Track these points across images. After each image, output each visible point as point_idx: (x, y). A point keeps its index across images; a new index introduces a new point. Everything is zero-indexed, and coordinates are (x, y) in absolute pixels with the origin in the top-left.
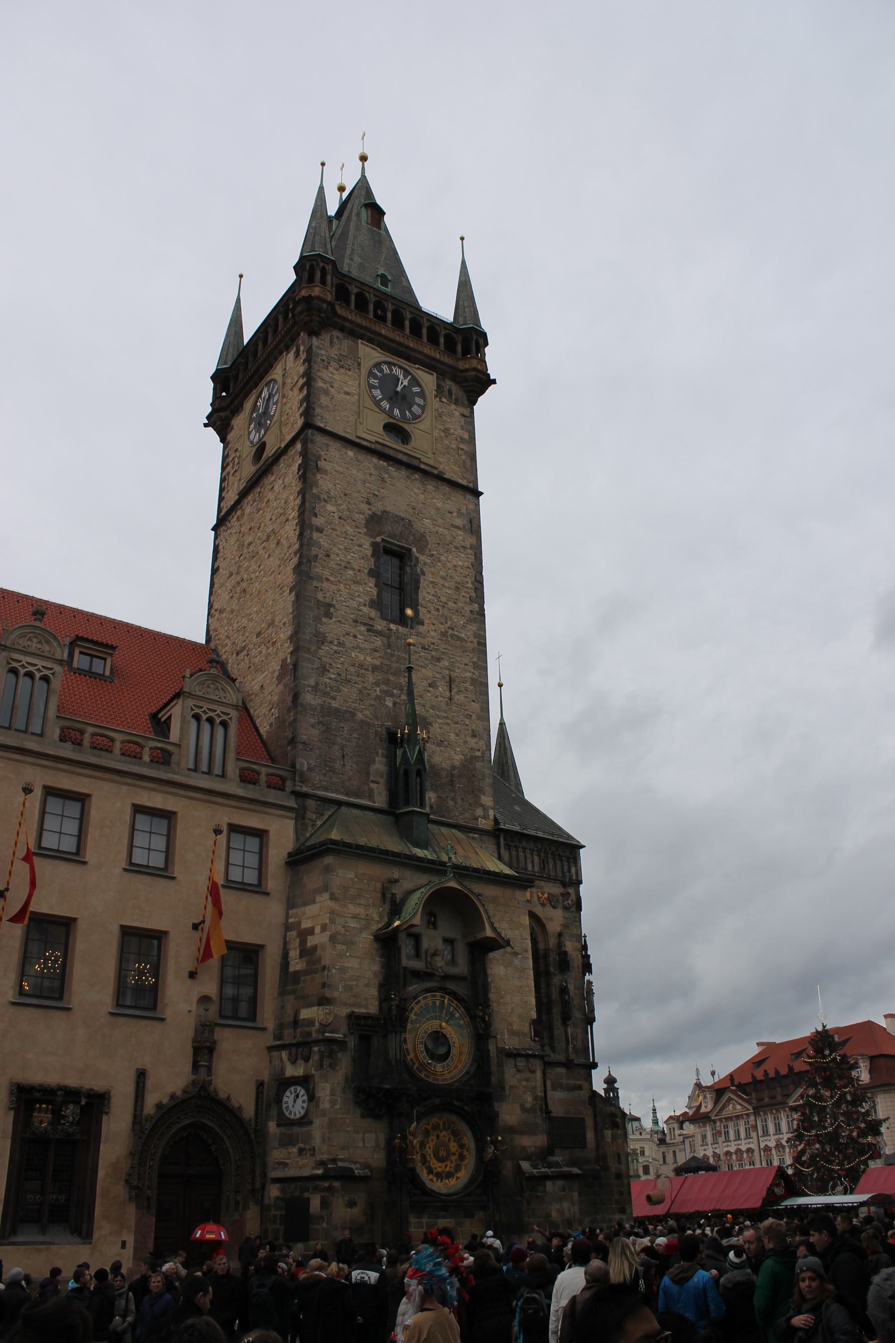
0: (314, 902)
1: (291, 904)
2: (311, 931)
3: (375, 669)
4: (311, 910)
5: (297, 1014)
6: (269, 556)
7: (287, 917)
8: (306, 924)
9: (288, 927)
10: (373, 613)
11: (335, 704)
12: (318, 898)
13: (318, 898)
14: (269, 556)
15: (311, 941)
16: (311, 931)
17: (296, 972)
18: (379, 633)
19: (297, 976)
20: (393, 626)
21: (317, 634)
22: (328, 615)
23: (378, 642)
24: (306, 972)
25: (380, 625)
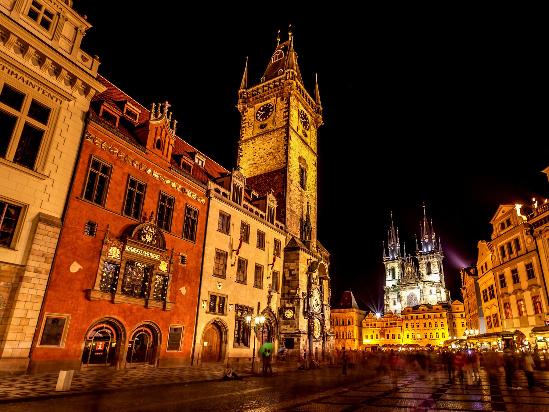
0: (294, 262)
1: (285, 261)
2: (294, 270)
3: (299, 200)
4: (293, 264)
5: (289, 291)
6: (270, 160)
7: (284, 265)
8: (291, 268)
9: (284, 268)
10: (299, 185)
11: (292, 209)
12: (296, 261)
13: (296, 261)
14: (270, 160)
15: (293, 273)
16: (294, 270)
17: (288, 280)
18: (300, 191)
19: (289, 281)
20: (302, 189)
21: (290, 188)
22: (292, 183)
23: (300, 193)
24: (292, 280)
25: (300, 188)
